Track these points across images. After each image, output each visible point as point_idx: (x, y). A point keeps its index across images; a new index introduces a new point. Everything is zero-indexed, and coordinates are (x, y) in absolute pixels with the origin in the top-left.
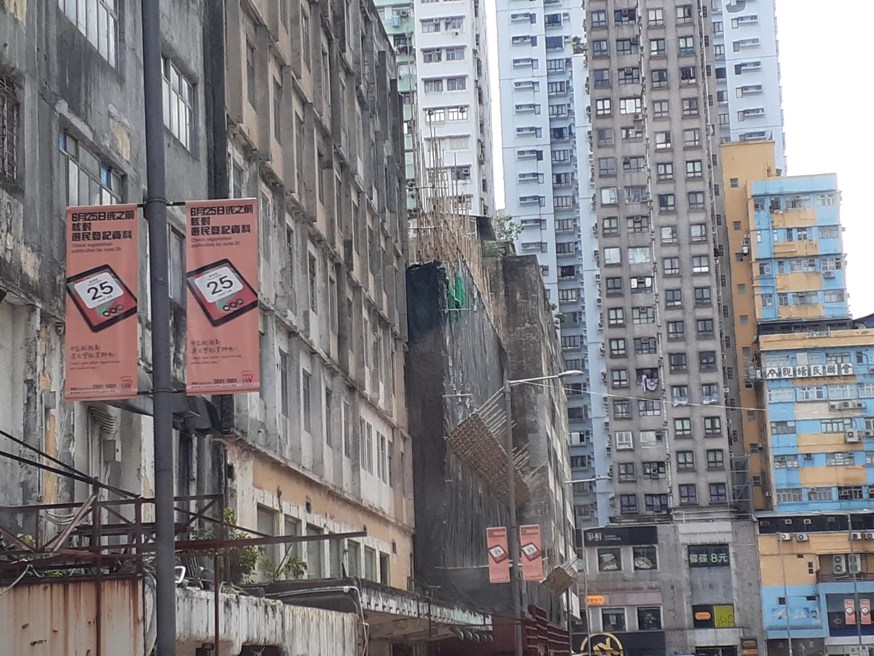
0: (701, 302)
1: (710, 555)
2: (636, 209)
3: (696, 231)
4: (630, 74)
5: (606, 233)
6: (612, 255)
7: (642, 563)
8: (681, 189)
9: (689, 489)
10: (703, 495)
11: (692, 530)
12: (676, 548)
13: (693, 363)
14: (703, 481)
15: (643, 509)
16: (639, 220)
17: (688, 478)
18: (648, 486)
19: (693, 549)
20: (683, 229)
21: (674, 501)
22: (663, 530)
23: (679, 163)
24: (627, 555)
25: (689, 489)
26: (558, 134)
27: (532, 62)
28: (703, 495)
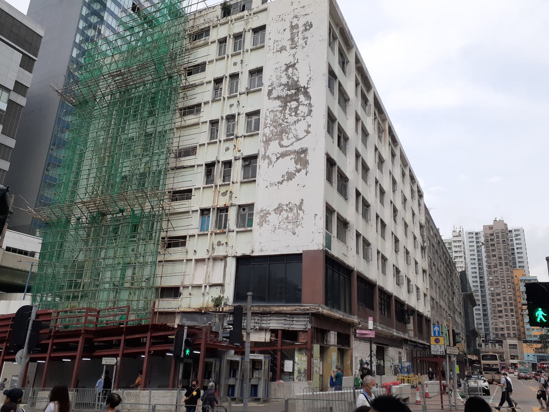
0: (510, 299)
1: (514, 346)
2: (496, 280)
3: (509, 286)
4: (494, 256)
5: (491, 284)
6: (492, 289)
7: (500, 347)
8: (505, 279)
9: (509, 334)
10: (512, 335)
11: (510, 341)
12: (507, 344)
13: (509, 311)
14: (512, 333)
15: (500, 336)
16: (497, 283)
17: (509, 332)
18: (501, 332)
19: (510, 345)
20: (506, 286)
21: (506, 336)
22: (504, 341)
23: (505, 274)
24: (497, 345)
25: (509, 334)
26: (481, 278)
27: (473, 246)
28: (512, 335)
